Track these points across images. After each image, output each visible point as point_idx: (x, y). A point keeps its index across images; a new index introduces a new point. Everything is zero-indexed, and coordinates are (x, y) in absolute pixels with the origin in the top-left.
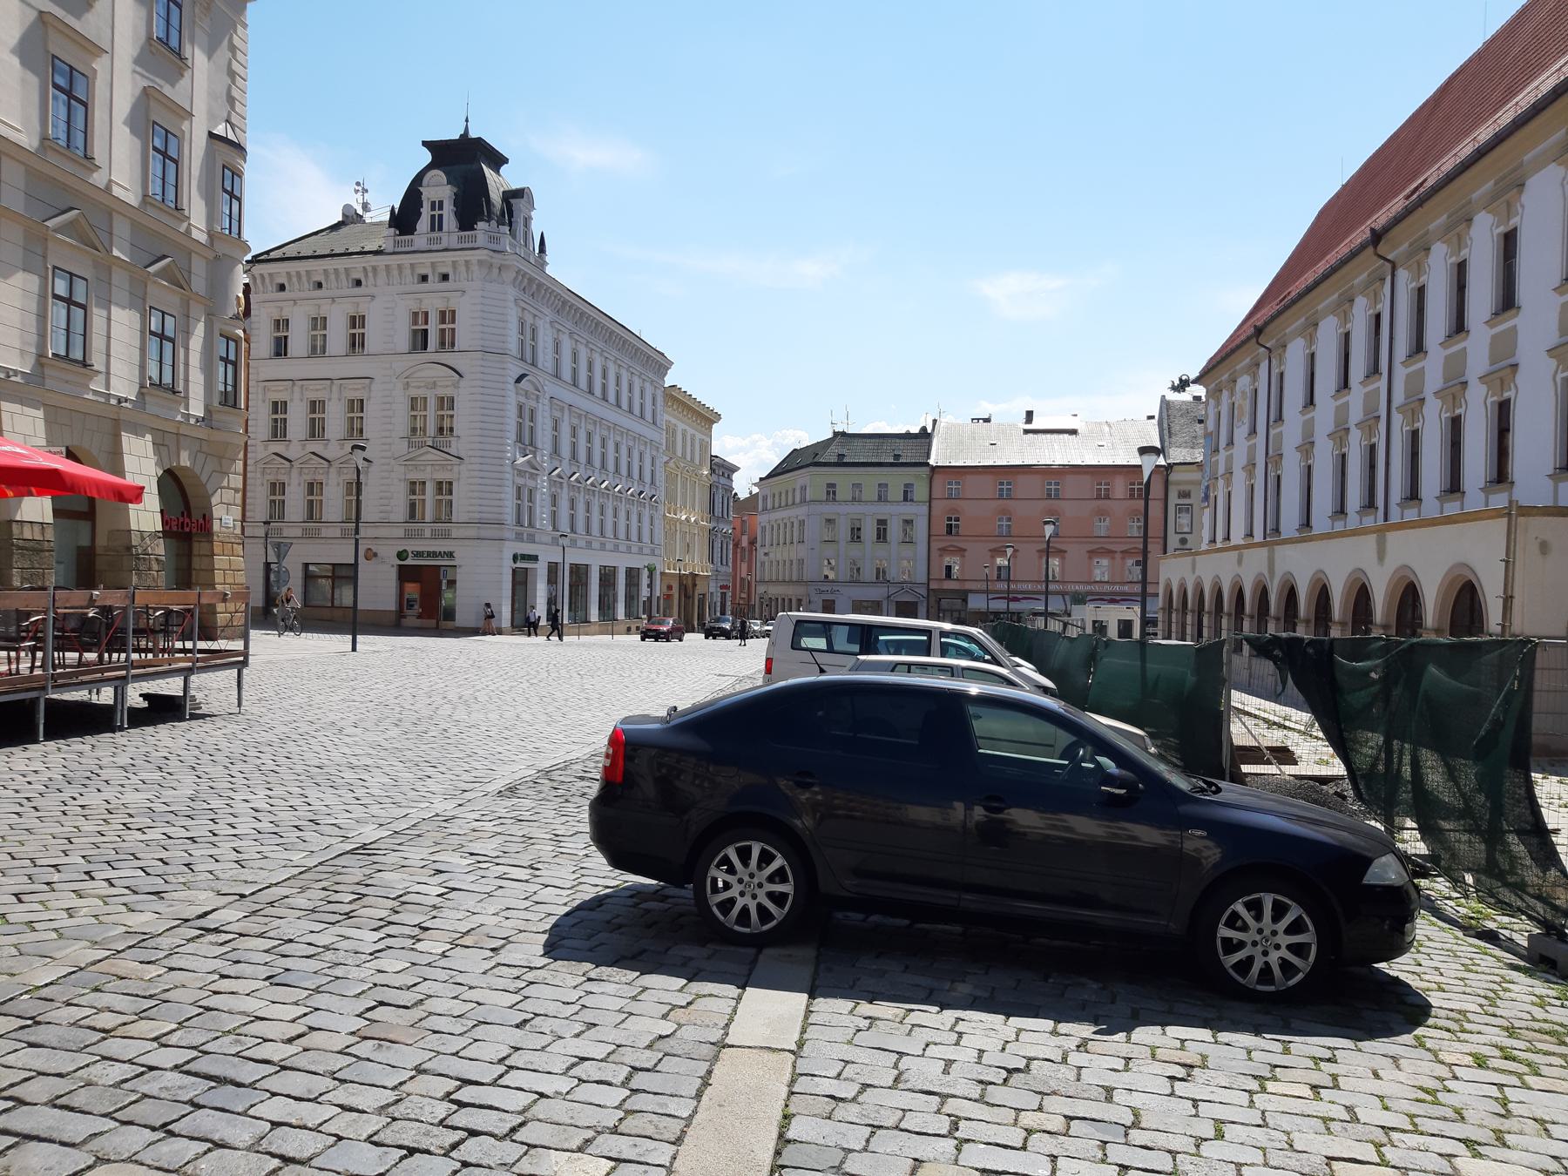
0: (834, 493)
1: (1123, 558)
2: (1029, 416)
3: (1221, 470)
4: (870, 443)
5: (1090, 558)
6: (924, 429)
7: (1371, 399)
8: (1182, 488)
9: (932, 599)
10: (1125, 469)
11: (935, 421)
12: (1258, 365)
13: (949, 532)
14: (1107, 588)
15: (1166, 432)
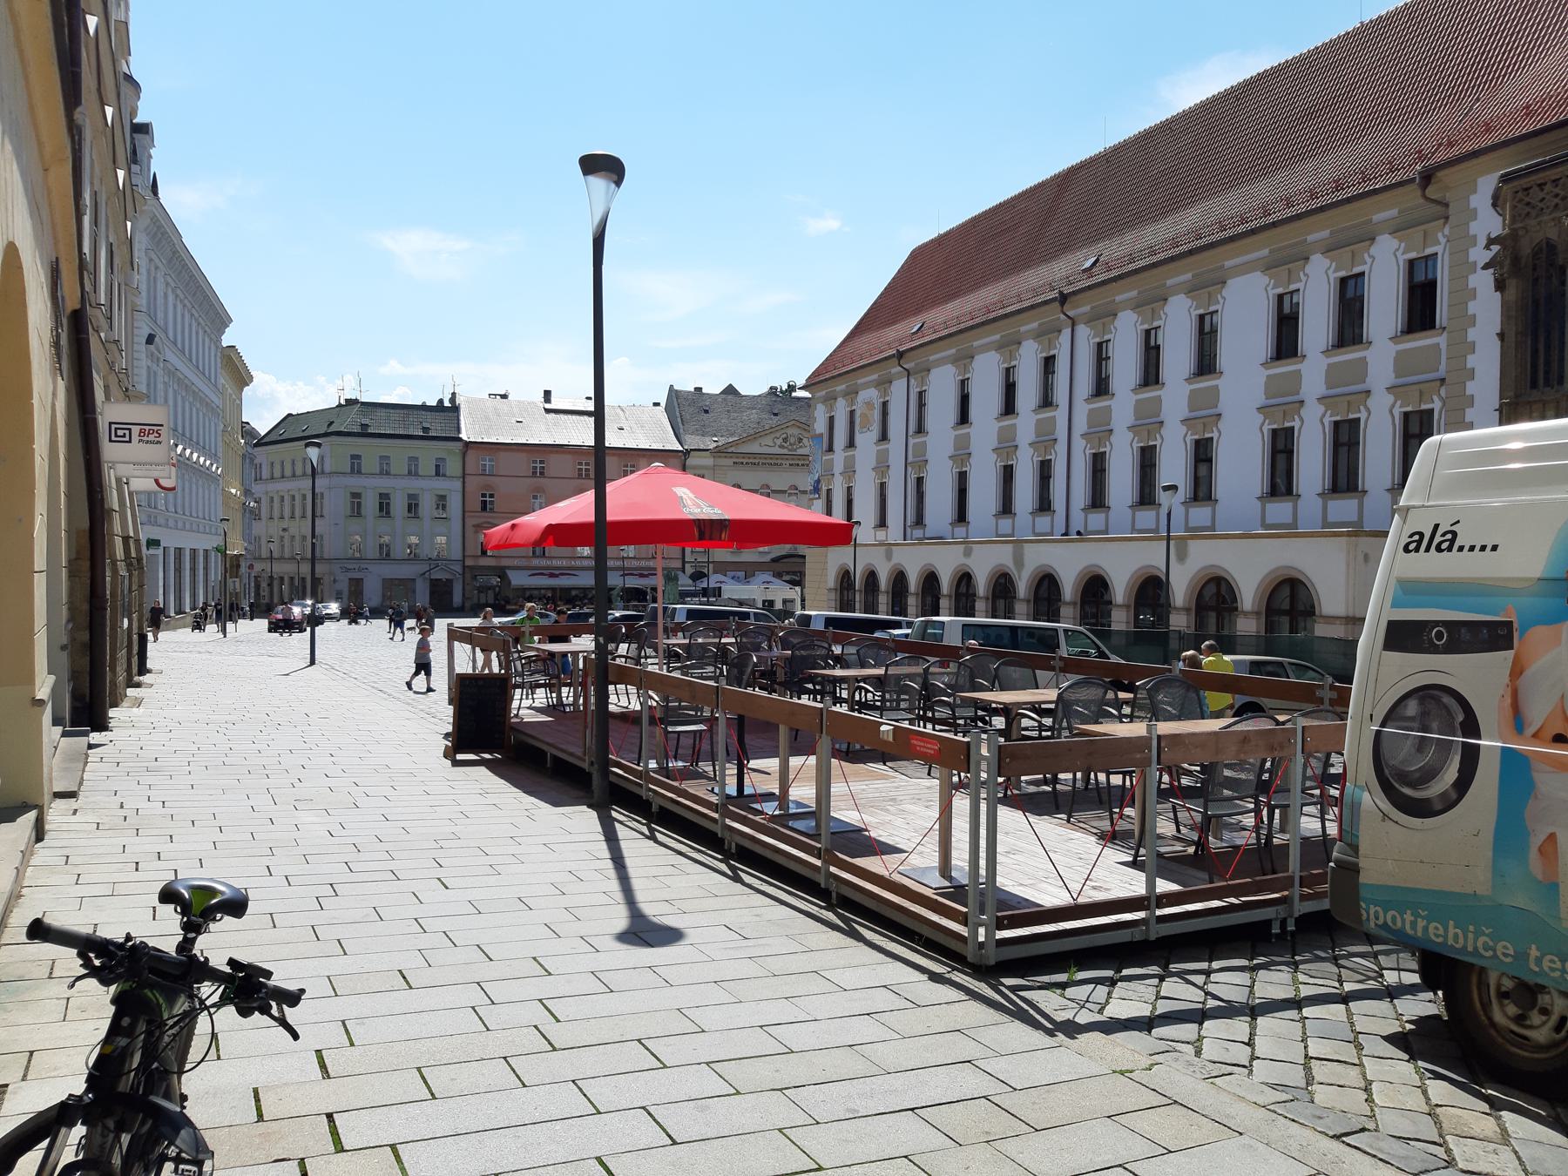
0: (359, 464)
2: (547, 395)
4: (395, 414)
6: (441, 401)
9: (468, 576)
10: (649, 453)
13: (484, 508)
14: (635, 563)
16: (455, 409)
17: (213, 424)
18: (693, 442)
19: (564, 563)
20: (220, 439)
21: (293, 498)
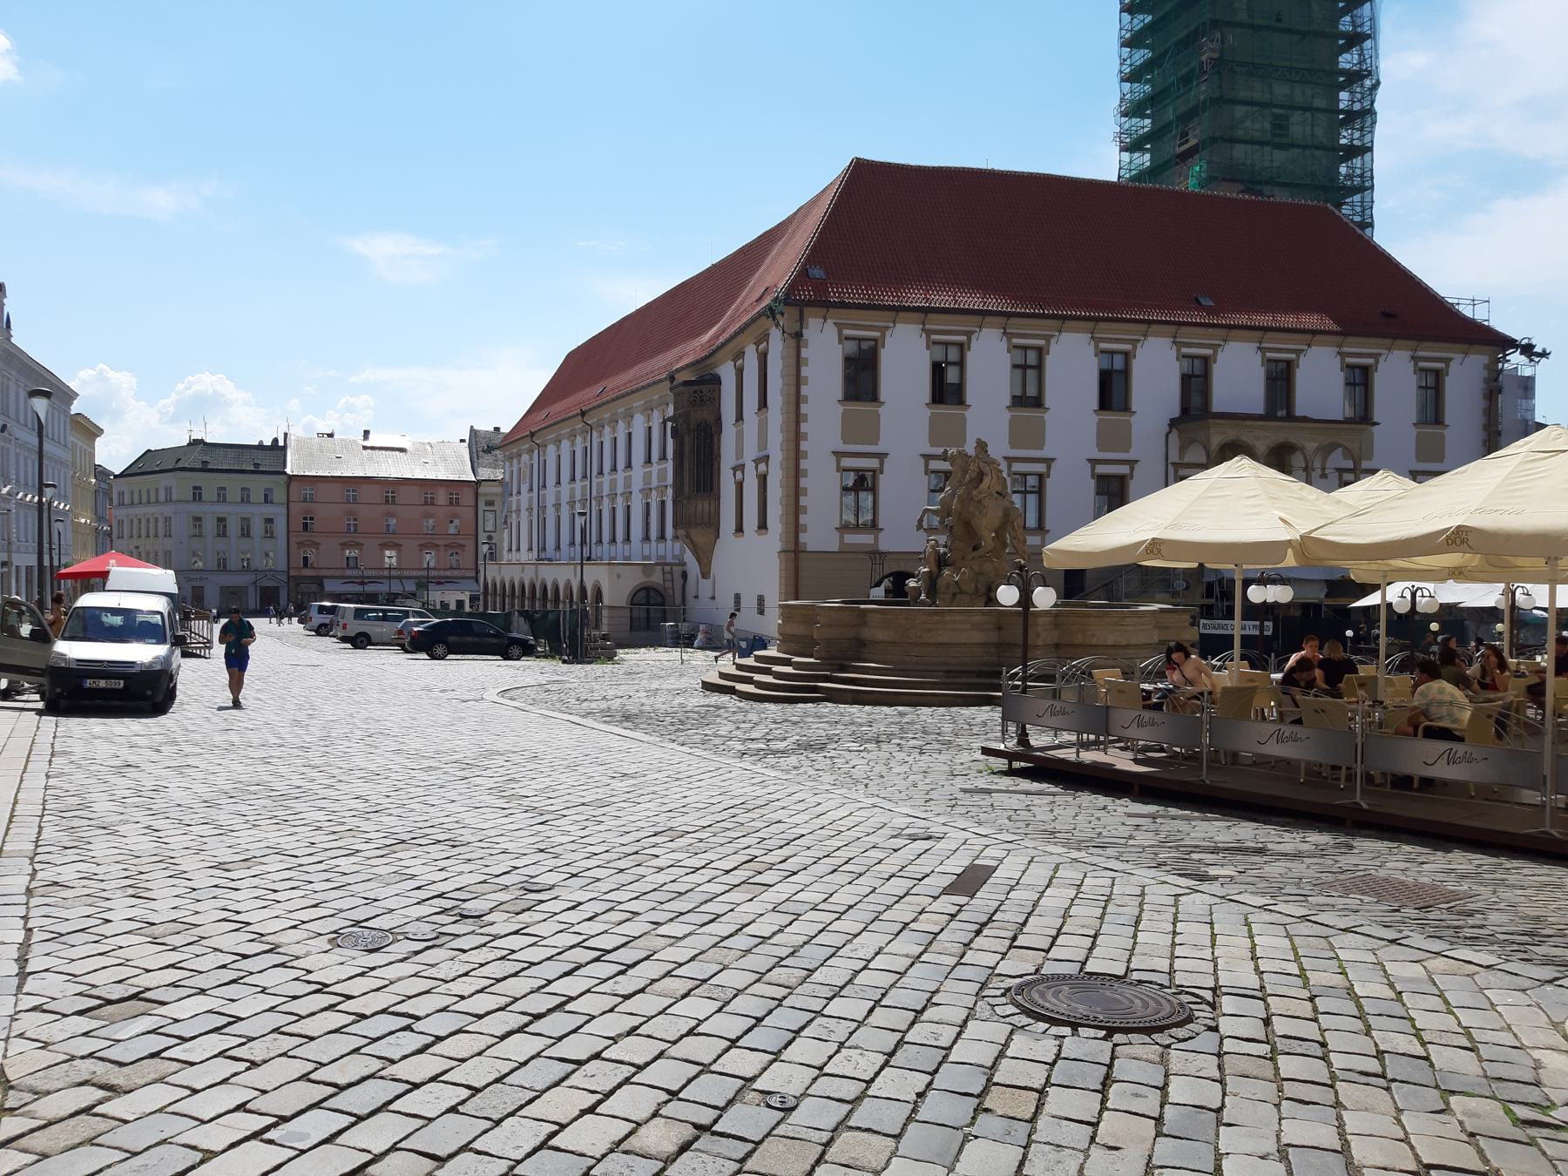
1: (446, 550)
2: (366, 433)
3: (514, 508)
5: (421, 550)
6: (276, 440)
7: (583, 487)
8: (489, 498)
9: (292, 584)
11: (286, 434)
12: (533, 451)
15: (475, 455)
16: (284, 448)
17: (62, 474)
18: (485, 473)
19: (374, 573)
20: (69, 482)
21: (148, 520)
